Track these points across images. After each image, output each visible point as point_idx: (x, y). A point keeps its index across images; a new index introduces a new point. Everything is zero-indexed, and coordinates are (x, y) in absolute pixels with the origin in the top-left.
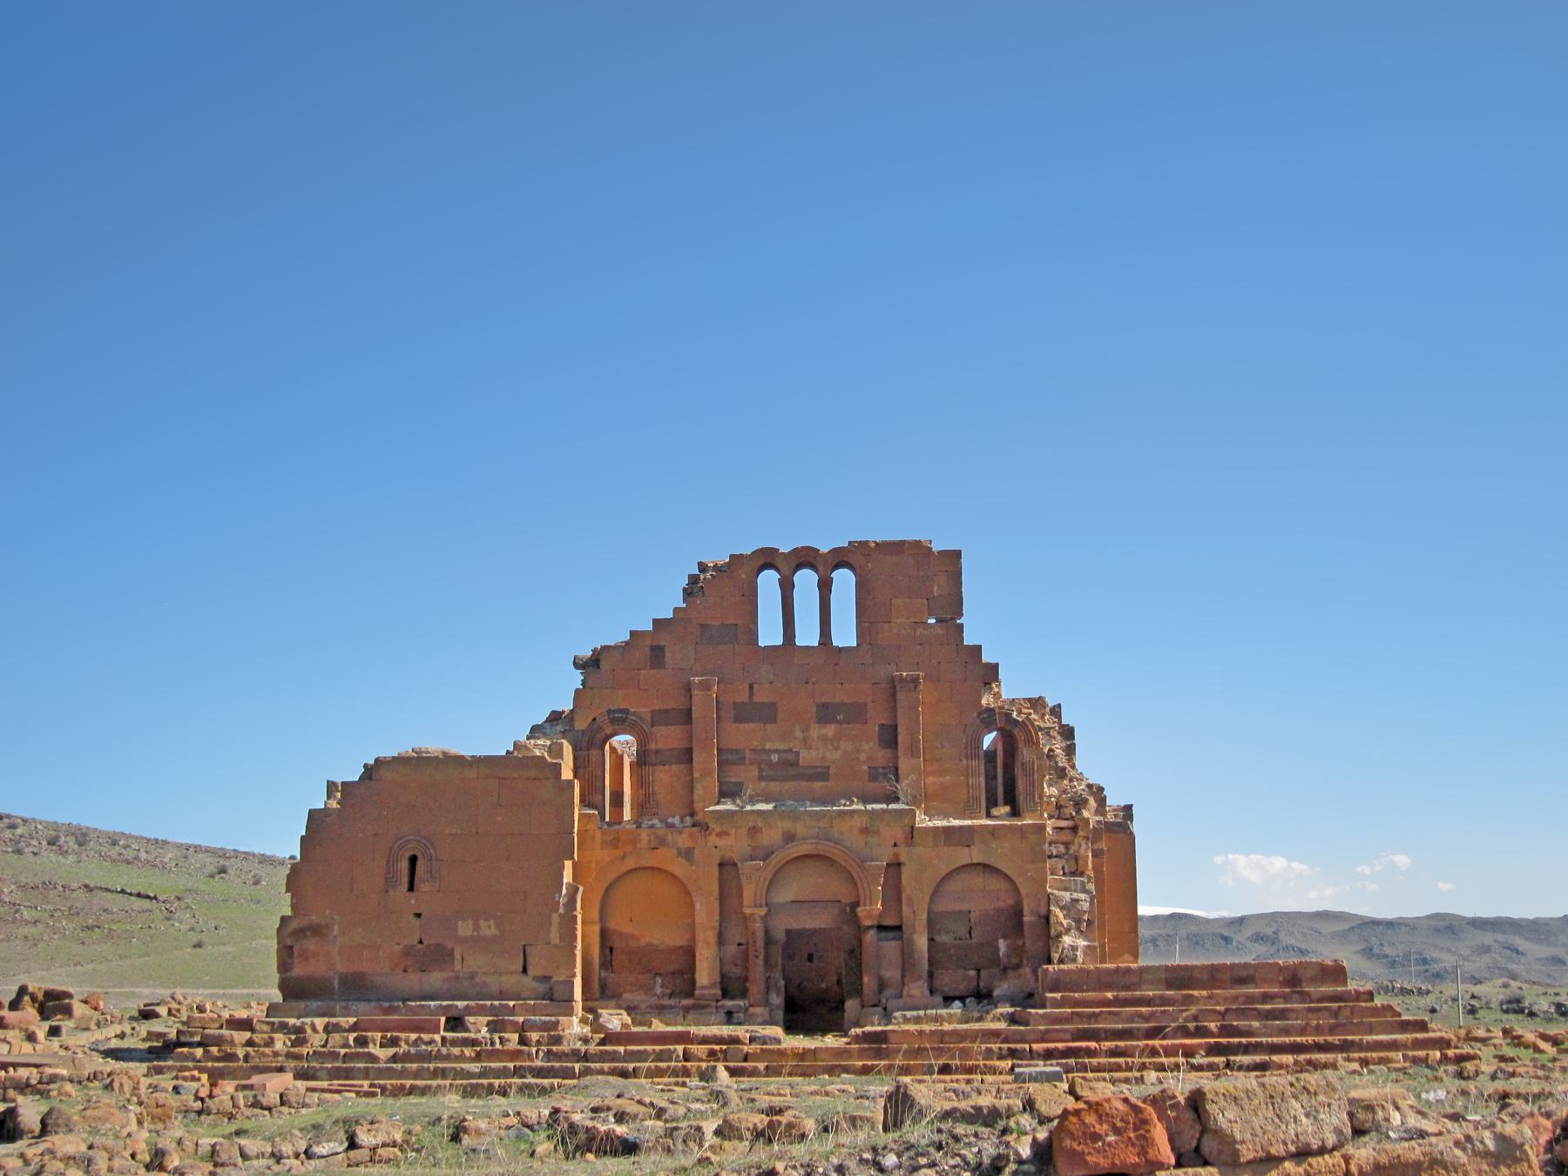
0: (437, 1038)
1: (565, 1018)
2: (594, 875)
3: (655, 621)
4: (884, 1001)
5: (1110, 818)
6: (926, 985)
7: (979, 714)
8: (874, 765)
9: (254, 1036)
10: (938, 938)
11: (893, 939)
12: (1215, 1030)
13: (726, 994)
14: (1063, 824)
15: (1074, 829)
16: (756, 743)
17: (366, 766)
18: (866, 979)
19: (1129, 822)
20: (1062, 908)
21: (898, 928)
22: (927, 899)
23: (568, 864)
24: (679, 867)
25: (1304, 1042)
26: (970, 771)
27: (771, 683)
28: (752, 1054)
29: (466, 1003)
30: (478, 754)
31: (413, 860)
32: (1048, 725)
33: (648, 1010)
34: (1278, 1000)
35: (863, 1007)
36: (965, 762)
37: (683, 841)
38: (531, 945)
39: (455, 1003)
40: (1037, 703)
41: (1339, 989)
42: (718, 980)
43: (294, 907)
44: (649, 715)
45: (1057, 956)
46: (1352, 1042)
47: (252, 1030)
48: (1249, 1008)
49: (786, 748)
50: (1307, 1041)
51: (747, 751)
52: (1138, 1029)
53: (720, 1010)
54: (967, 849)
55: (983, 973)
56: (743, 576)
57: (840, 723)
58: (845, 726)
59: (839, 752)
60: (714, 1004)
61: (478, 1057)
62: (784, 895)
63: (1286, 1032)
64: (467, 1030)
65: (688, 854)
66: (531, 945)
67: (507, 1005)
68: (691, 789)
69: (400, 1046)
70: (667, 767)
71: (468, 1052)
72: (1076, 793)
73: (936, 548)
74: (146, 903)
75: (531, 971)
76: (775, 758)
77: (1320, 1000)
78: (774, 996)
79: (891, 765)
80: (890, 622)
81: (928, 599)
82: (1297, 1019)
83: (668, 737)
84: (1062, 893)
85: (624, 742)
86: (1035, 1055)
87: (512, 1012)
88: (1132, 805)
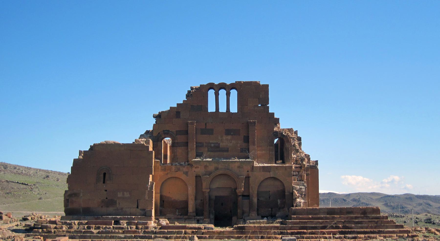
0: (111, 227)
1: (149, 221)
2: (158, 179)
3: (178, 104)
4: (244, 217)
5: (311, 164)
6: (256, 213)
7: (273, 133)
9: (57, 226)
10: (260, 199)
11: (247, 199)
12: (341, 227)
13: (197, 215)
14: (298, 166)
15: (301, 167)
16: (207, 141)
17: (91, 146)
18: (239, 211)
19: (317, 166)
20: (297, 191)
21: (248, 196)
22: (257, 187)
23: (151, 176)
24: (183, 177)
25: (367, 231)
26: (270, 150)
27: (212, 123)
28: (205, 232)
29: (120, 216)
30: (124, 143)
31: (105, 174)
32: (294, 136)
33: (174, 219)
34: (359, 218)
35: (238, 219)
36: (269, 147)
37: (185, 169)
38: (140, 200)
39: (117, 216)
40: (290, 130)
41: (378, 215)
42: (195, 210)
43: (69, 188)
45: (295, 205)
46: (381, 231)
47: (56, 224)
48: (351, 221)
49: (216, 142)
50: (368, 230)
51: (204, 143)
52: (319, 226)
53: (195, 219)
54: (269, 173)
55: (273, 210)
56: (204, 91)
57: (232, 135)
59: (232, 143)
60: (194, 218)
61: (123, 233)
62: (215, 185)
63: (362, 228)
64: (120, 225)
65: (186, 173)
66: (140, 200)
67: (132, 217)
68: (188, 154)
69: (100, 229)
70: (181, 148)
71: (120, 231)
72: (301, 157)
73: (261, 83)
74: (25, 186)
75: (140, 207)
76: (212, 145)
77: (372, 219)
79: (247, 148)
80: (247, 105)
81: (259, 99)
82: (365, 224)
83: (181, 139)
84: (297, 186)
85: (168, 140)
86: (288, 234)
87: (134, 219)
88: (318, 161)
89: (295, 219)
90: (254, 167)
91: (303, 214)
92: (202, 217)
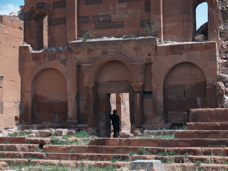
6: (162, 118)
8: (142, 20)
10: (169, 97)
13: (79, 123)
16: (94, 13)
22: (163, 79)
24: (60, 67)
26: (184, 20)
44: (52, 5)
49: (106, 14)
54: (181, 55)
58: (130, 2)
59: (128, 14)
60: (74, 126)
65: (64, 62)
70: (59, 26)
76: (101, 19)
78: (101, 123)
89: (190, 127)
90: (157, 48)
91: (209, 120)
92: (85, 126)
